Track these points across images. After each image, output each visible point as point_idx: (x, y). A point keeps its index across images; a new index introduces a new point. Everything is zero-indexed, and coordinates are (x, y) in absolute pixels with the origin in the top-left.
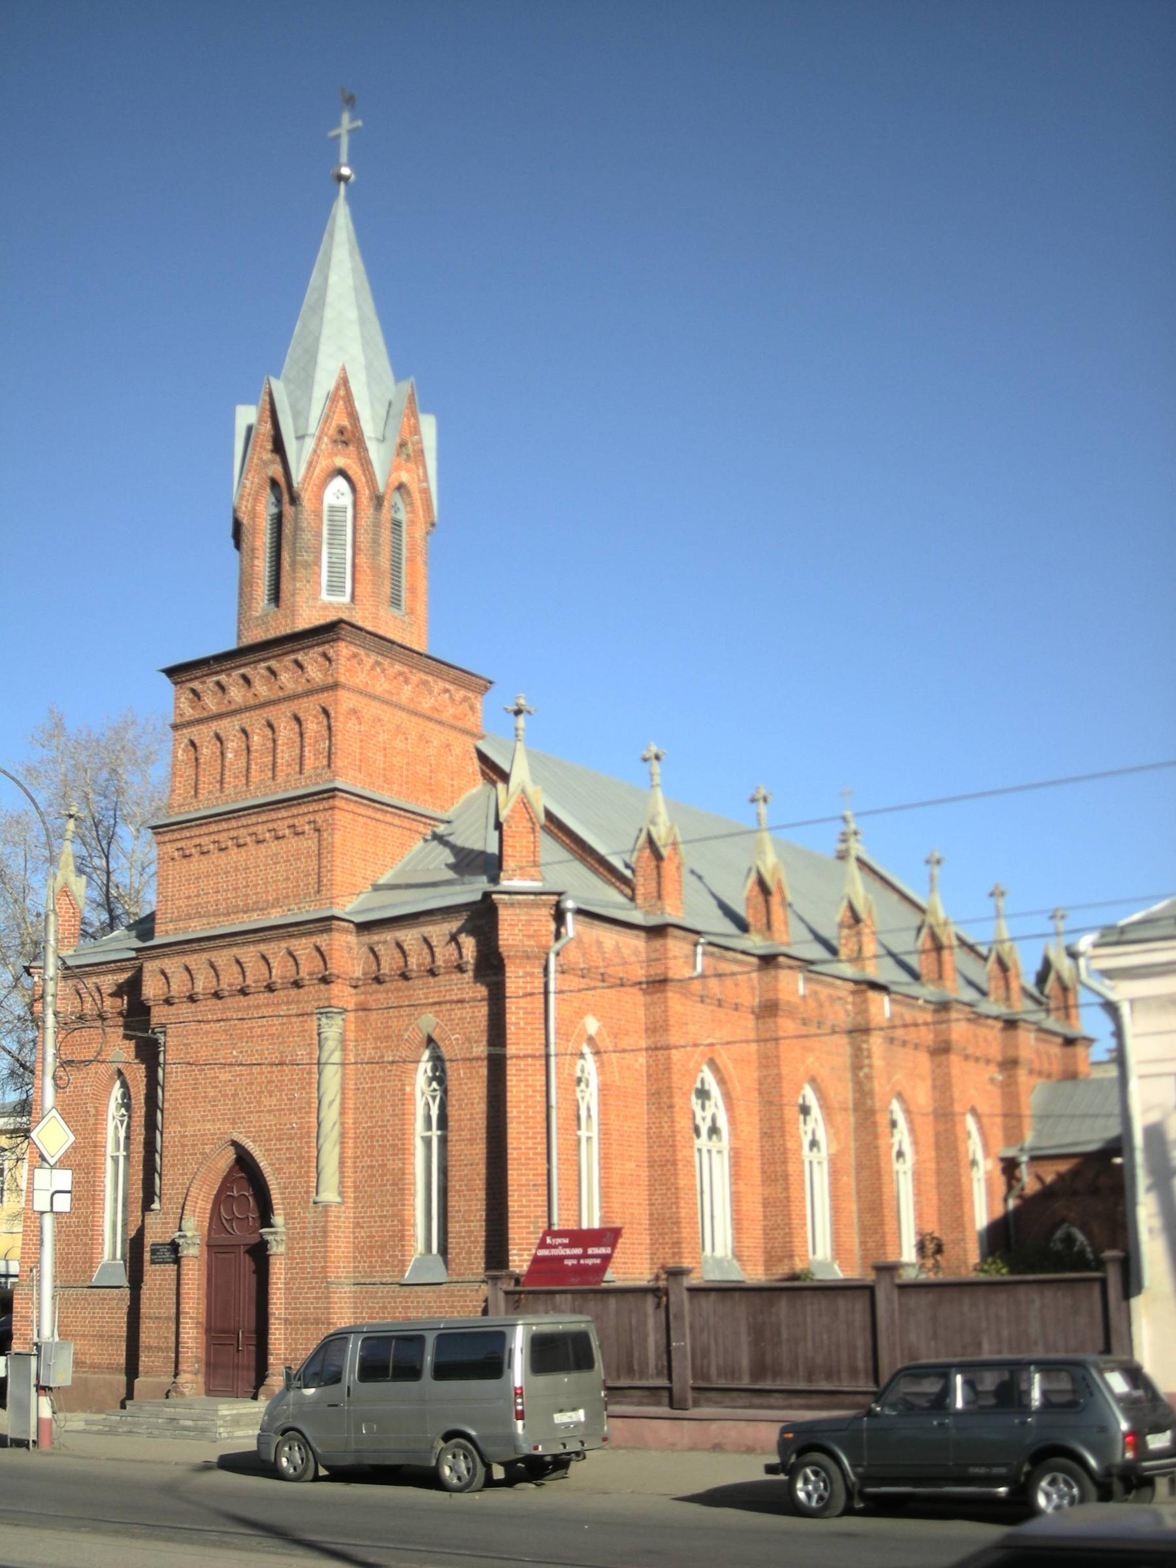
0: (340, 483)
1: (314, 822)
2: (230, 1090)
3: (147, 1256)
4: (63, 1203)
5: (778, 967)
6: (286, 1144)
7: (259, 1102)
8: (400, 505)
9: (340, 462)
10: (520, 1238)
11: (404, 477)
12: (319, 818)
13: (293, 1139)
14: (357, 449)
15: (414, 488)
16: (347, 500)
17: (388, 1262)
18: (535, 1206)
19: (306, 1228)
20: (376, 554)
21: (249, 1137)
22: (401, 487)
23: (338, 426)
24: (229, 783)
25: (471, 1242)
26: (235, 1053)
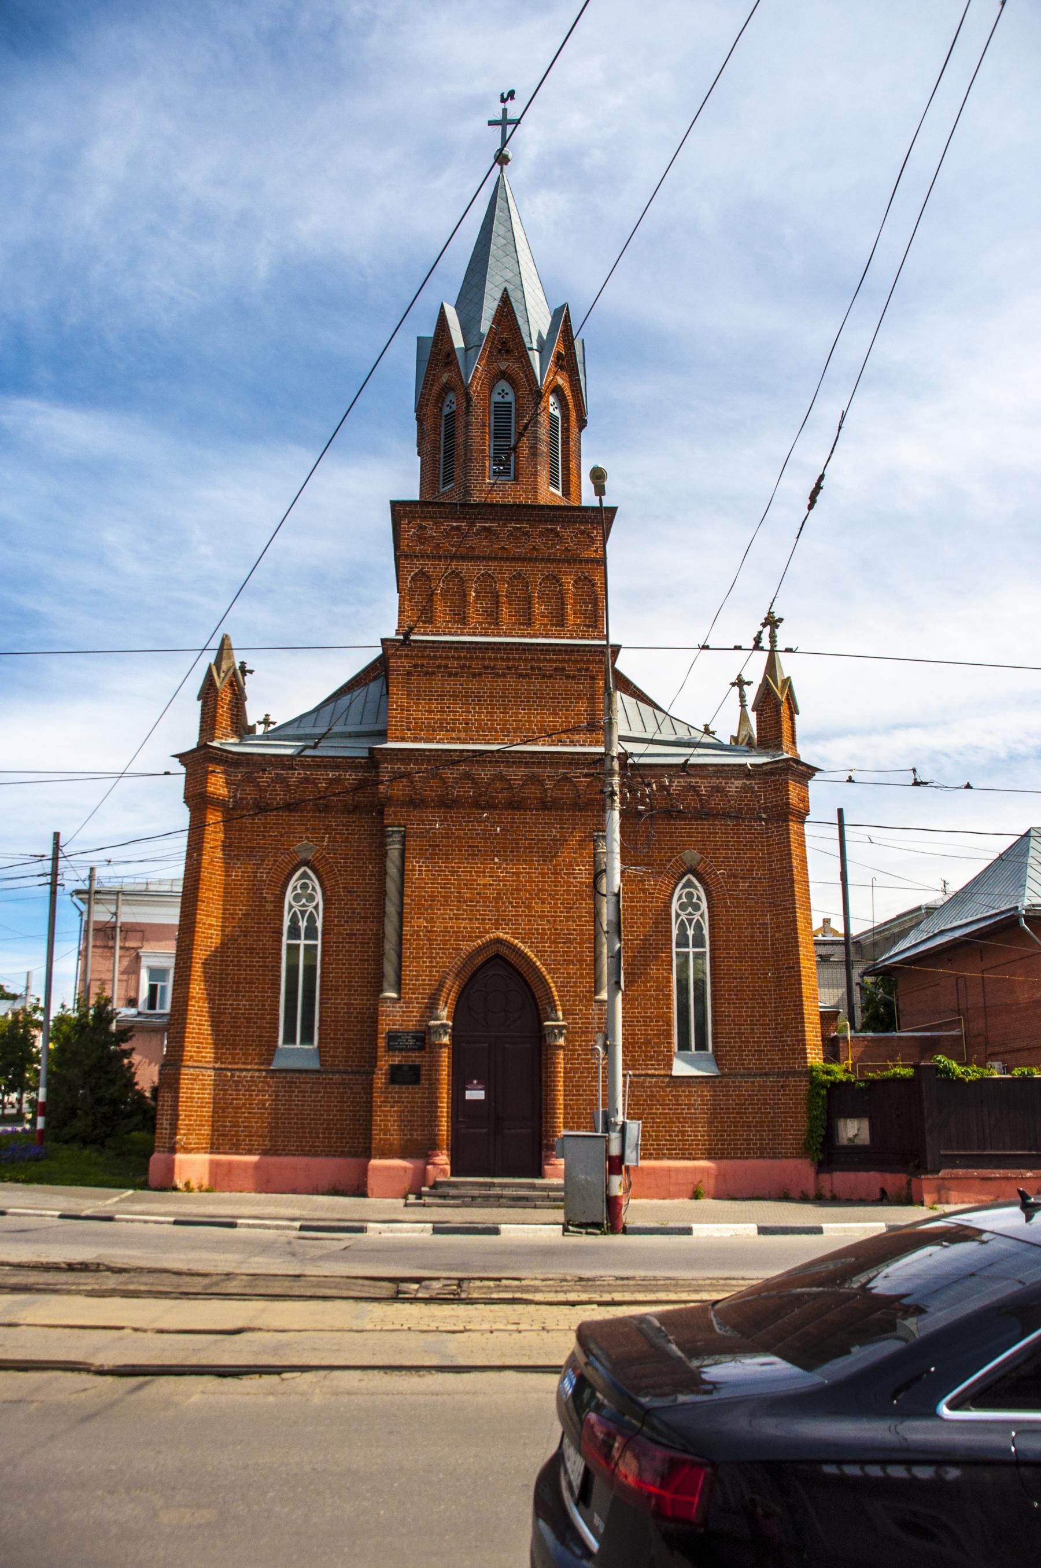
1: (587, 670)
2: (491, 894)
3: (382, 1043)
6: (562, 948)
7: (529, 907)
13: (572, 943)
17: (652, 1057)
19: (590, 1023)
21: (517, 938)
24: (473, 618)
25: (742, 1042)
26: (496, 860)
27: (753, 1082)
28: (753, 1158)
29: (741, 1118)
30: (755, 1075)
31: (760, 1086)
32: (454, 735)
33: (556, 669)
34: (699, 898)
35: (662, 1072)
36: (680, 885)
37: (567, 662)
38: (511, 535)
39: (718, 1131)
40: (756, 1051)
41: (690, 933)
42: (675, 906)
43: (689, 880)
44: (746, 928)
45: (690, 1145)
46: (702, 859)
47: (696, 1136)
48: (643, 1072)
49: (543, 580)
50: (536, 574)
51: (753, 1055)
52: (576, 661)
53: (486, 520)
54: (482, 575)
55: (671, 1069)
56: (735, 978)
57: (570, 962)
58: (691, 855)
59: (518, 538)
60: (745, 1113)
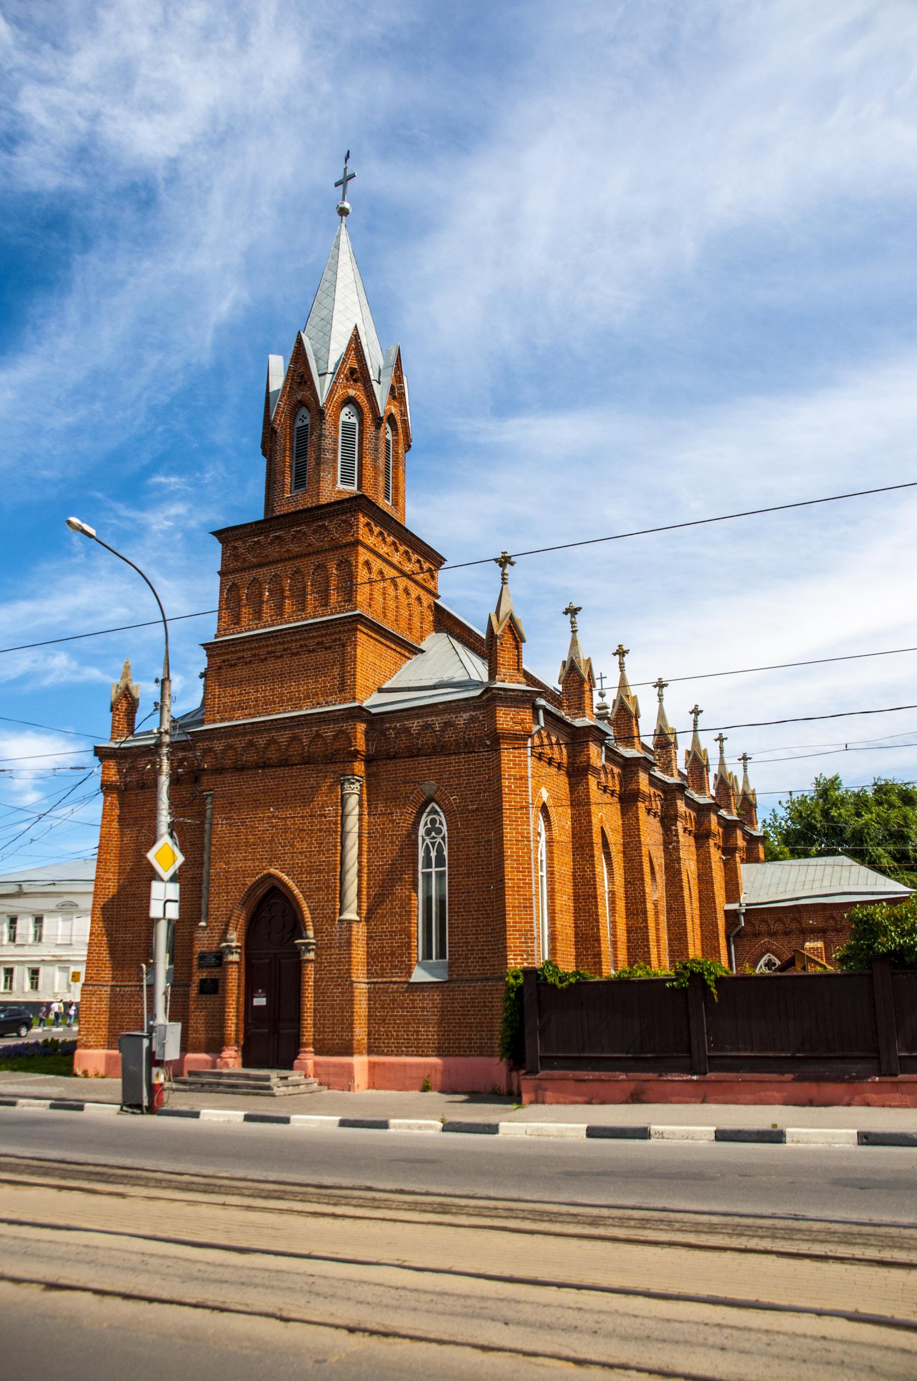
0: (346, 410)
1: (340, 639)
3: (195, 962)
4: (173, 912)
5: (639, 765)
6: (315, 877)
7: (292, 846)
8: (389, 429)
9: (352, 392)
10: (515, 947)
11: (394, 410)
12: (344, 637)
13: (321, 873)
14: (364, 385)
15: (398, 418)
16: (354, 420)
17: (396, 966)
18: (525, 923)
19: (333, 940)
20: (375, 460)
21: (283, 872)
22: (391, 419)
23: (350, 368)
24: (267, 613)
25: (468, 950)
26: (272, 809)
27: (475, 987)
28: (473, 1055)
29: (465, 1019)
30: (478, 980)
31: (480, 990)
32: (247, 712)
33: (318, 644)
34: (441, 823)
35: (403, 979)
36: (425, 815)
37: (325, 636)
38: (295, 537)
39: (445, 1031)
40: (479, 958)
41: (433, 854)
42: (422, 831)
43: (433, 807)
44: (474, 847)
45: (423, 1043)
46: (439, 788)
47: (427, 1035)
48: (389, 980)
49: (315, 569)
50: (308, 565)
51: (477, 962)
52: (331, 634)
53: (276, 530)
54: (274, 576)
55: (410, 976)
56: (463, 893)
57: (319, 889)
58: (430, 786)
59: (300, 539)
60: (467, 1015)
